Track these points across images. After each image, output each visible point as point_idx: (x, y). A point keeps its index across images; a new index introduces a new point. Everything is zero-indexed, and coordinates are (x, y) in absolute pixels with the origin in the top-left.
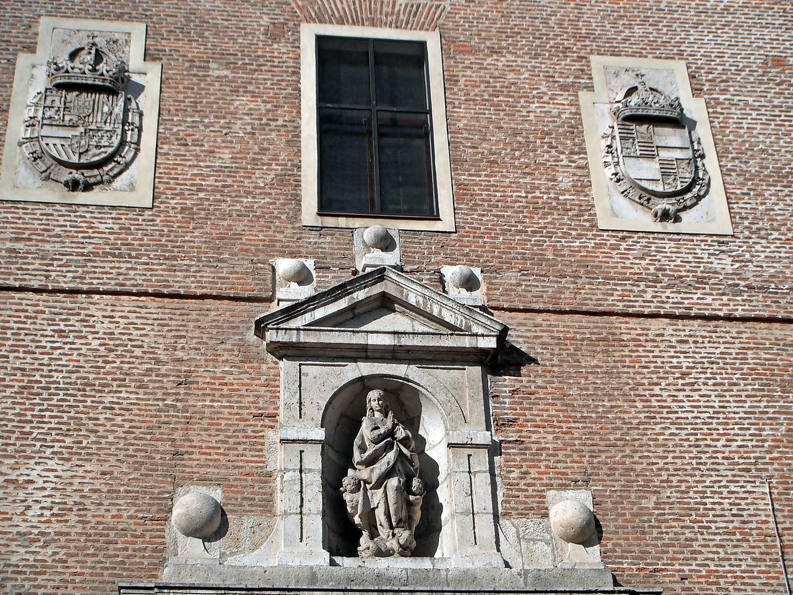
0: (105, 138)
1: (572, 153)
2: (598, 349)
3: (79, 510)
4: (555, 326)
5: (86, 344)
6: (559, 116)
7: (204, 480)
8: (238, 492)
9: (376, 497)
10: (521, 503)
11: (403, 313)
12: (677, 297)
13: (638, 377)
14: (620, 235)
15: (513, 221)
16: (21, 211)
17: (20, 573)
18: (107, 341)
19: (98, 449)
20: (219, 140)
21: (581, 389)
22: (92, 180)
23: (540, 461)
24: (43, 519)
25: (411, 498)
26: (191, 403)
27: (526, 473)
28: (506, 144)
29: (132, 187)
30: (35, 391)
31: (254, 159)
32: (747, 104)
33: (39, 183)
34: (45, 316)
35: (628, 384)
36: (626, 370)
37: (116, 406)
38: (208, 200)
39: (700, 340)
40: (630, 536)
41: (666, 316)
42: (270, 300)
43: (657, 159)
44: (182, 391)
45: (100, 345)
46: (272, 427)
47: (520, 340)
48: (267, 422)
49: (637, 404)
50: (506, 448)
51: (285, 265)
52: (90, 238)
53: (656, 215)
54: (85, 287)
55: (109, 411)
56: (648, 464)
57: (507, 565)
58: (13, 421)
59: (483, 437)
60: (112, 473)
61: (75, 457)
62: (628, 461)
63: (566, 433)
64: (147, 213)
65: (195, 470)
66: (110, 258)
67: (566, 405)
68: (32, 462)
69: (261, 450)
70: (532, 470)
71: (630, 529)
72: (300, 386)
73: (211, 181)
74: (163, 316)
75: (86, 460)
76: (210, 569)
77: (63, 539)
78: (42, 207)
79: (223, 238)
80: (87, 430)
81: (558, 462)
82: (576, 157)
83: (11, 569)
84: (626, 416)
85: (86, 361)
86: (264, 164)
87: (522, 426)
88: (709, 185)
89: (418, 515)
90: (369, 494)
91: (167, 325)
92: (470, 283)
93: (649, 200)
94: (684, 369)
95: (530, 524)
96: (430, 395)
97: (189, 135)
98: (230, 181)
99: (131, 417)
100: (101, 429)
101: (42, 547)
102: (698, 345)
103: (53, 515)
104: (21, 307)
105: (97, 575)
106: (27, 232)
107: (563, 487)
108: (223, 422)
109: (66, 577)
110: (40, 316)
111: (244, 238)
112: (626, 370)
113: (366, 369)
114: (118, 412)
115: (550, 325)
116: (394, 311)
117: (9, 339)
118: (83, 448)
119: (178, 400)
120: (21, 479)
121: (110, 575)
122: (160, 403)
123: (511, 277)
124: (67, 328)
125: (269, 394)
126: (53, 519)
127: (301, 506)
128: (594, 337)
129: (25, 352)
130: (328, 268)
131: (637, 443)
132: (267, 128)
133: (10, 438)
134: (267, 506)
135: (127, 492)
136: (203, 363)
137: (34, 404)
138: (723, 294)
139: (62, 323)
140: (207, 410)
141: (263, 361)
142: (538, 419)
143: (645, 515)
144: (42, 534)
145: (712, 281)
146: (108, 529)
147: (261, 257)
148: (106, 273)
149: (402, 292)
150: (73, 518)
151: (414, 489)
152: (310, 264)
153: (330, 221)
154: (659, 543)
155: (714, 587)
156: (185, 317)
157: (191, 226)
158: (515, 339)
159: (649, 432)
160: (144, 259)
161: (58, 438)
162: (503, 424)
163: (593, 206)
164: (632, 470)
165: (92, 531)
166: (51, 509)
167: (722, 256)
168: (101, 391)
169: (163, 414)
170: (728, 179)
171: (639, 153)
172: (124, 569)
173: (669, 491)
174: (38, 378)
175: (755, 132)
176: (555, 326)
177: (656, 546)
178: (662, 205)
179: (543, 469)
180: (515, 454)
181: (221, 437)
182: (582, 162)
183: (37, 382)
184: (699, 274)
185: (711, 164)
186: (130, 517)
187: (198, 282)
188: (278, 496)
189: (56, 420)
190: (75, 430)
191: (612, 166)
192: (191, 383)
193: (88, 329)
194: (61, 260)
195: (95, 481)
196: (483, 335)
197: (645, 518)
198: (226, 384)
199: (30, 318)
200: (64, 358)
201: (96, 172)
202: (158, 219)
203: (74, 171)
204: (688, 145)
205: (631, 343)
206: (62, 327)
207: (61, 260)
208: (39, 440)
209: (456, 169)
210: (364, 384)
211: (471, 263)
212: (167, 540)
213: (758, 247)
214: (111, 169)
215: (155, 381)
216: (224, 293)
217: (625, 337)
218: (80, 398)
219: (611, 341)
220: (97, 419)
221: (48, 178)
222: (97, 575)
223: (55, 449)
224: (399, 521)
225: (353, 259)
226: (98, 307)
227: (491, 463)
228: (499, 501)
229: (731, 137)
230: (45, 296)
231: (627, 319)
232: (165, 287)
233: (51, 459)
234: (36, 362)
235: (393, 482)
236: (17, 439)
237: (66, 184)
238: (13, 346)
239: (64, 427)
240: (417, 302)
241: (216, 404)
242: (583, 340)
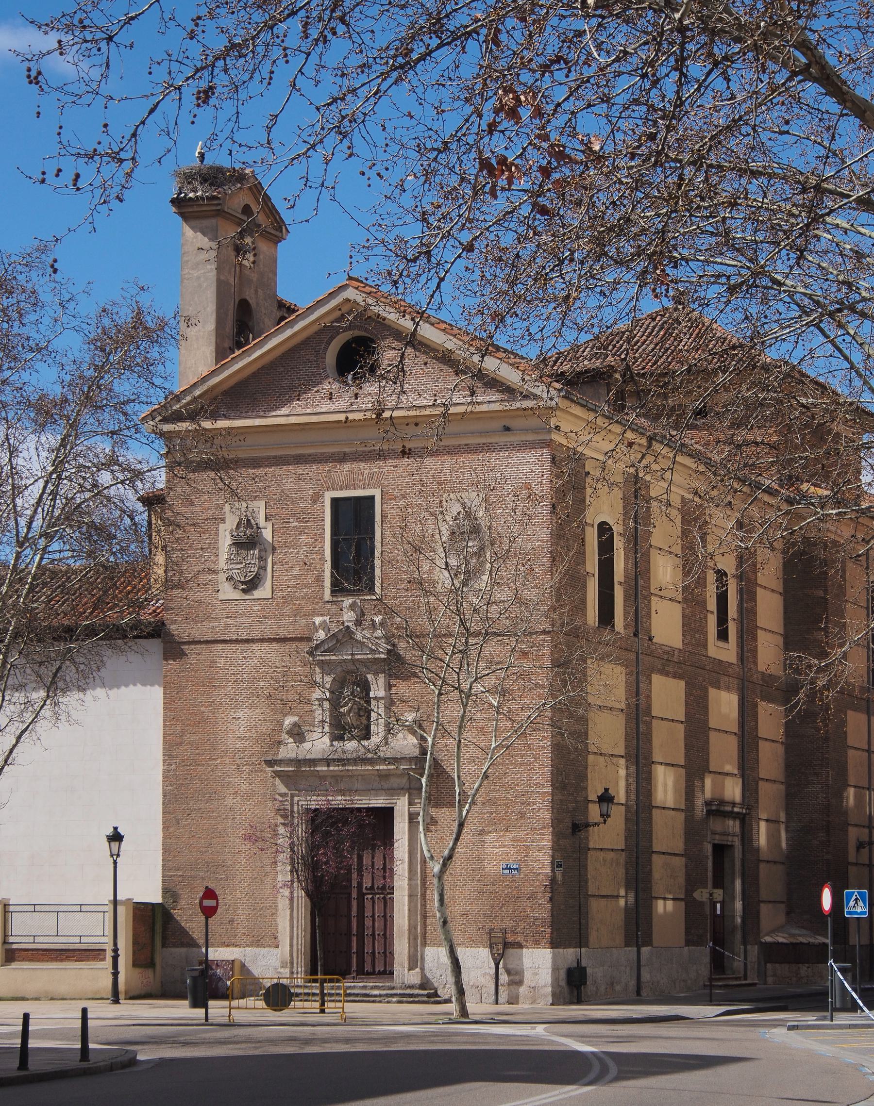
33: (233, 590)
150: (254, 731)
153: (335, 599)
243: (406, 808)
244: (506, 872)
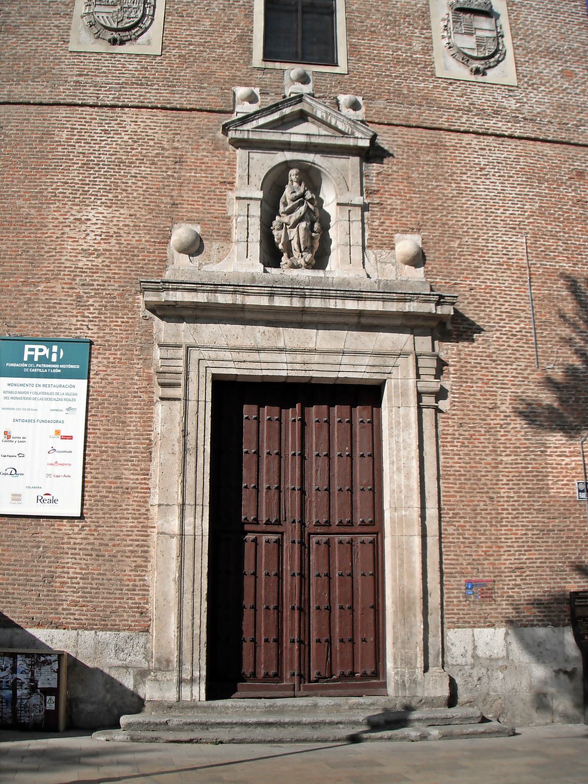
0: (133, 13)
1: (422, 29)
2: (431, 150)
3: (117, 236)
4: (406, 135)
5: (121, 138)
6: (416, 5)
7: (190, 220)
8: (210, 228)
9: (293, 233)
10: (379, 240)
11: (313, 122)
12: (481, 122)
13: (454, 168)
14: (449, 81)
15: (384, 69)
16: (82, 58)
17: (83, 272)
18: (133, 136)
19: (128, 201)
20: (203, 13)
21: (420, 174)
22: (125, 38)
23: (392, 216)
24: (96, 242)
25: (313, 234)
26: (183, 174)
27: (383, 223)
28: (381, 21)
29: (149, 43)
30: (91, 166)
31: (224, 26)
32: (531, 6)
33: (93, 40)
34: (96, 121)
35: (447, 172)
36: (447, 164)
37: (138, 175)
38: (195, 50)
39: (493, 149)
40: (442, 263)
41: (473, 133)
42: (232, 112)
43: (475, 36)
44: (177, 167)
45: (129, 138)
46: (231, 190)
47: (384, 142)
48: (228, 186)
49: (453, 185)
50: (372, 207)
51: (241, 91)
52: (123, 73)
53: (471, 71)
54: (120, 104)
55: (134, 179)
56: (456, 221)
57: (368, 276)
58: (78, 184)
59: (358, 200)
60: (136, 215)
61: (114, 206)
62: (444, 218)
63: (408, 200)
64: (158, 58)
65: (185, 214)
66: (135, 86)
67: (410, 183)
68: (89, 208)
69: (224, 203)
70: (387, 221)
71: (442, 259)
72: (249, 165)
73: (197, 39)
74: (167, 122)
75: (120, 207)
76: (193, 272)
77: (107, 253)
78: (95, 55)
79: (204, 74)
80: (121, 190)
81: (403, 217)
82: (425, 31)
83: (78, 270)
84: (445, 192)
85: (120, 148)
86: (230, 29)
87: (382, 194)
88: (505, 54)
89: (317, 245)
90: (288, 231)
91: (169, 127)
92: (355, 106)
93: (468, 61)
94: (482, 166)
96: (327, 174)
97: (184, 10)
98: (209, 39)
99: (147, 182)
100: (129, 189)
101: (96, 258)
103: (102, 239)
104: (82, 116)
105: (127, 274)
106: (86, 71)
107: (405, 232)
108: (202, 186)
109: (110, 275)
110: (94, 121)
111: (217, 74)
112: (447, 164)
113: (289, 156)
114: (139, 179)
115: (403, 134)
116: (308, 121)
117: (75, 135)
118: (118, 200)
119: (175, 172)
120: (83, 218)
121: (135, 275)
122: (164, 174)
123: (380, 103)
124: (109, 129)
125: (229, 170)
126: (102, 241)
127: (247, 237)
128: (429, 143)
129: (85, 143)
130: (268, 94)
131: (450, 208)
132: (233, 6)
133: (76, 194)
134: (227, 236)
135: (144, 226)
136: (190, 150)
137: (90, 174)
138: (509, 122)
139: (106, 126)
140: (192, 179)
141: (227, 149)
142: (392, 190)
143: (452, 251)
144: (96, 250)
145: (503, 113)
146: (134, 248)
147: (227, 86)
148: (133, 95)
149: (313, 110)
150: (113, 241)
151: (315, 229)
152: (257, 91)
153: (270, 65)
154: (459, 268)
155: (488, 295)
156: (180, 122)
157: (185, 66)
158: (383, 142)
159: (458, 202)
160: (155, 87)
161: (104, 194)
162: (371, 193)
163: (433, 62)
164: (446, 224)
165: (125, 249)
166: (101, 236)
167: (510, 98)
168: (129, 166)
169: (166, 180)
170: (517, 51)
171: (463, 31)
172: (143, 271)
173: (467, 237)
174: (92, 158)
175: (535, 24)
176: (406, 135)
177: (457, 269)
178: (476, 64)
179: (393, 221)
180: (377, 211)
181: (201, 195)
182: (428, 35)
183: (91, 161)
184: (496, 109)
185: (507, 42)
186: (147, 241)
187: (188, 101)
188: (234, 231)
189: (103, 183)
190: (114, 189)
191: (447, 39)
192: (183, 162)
193: (122, 129)
194: (106, 87)
195: (126, 220)
196: (361, 138)
197: (452, 253)
198: (204, 163)
199: (88, 122)
200: (108, 146)
201: (127, 33)
202: (165, 62)
203: (114, 33)
204: (494, 28)
205: (452, 148)
206: (106, 128)
207: (106, 87)
208: (93, 195)
209: (350, 35)
210: (287, 165)
211: (357, 94)
212: (168, 255)
213: (532, 95)
214: (137, 32)
215: (161, 161)
216: (204, 107)
217: (448, 144)
218: (117, 170)
219: (439, 146)
220: (127, 183)
221: (98, 37)
222: (127, 274)
223: (103, 201)
224: (305, 248)
225: (283, 88)
226: (128, 116)
227: (363, 216)
228: (366, 239)
229: (521, 26)
230: (96, 109)
231: (450, 133)
232: (168, 103)
233: (101, 206)
234: (91, 149)
235: (303, 225)
236: (81, 194)
237: (109, 41)
238: (78, 139)
239: (108, 188)
240: (322, 116)
241: (197, 175)
242: (422, 144)
243: (412, 382)
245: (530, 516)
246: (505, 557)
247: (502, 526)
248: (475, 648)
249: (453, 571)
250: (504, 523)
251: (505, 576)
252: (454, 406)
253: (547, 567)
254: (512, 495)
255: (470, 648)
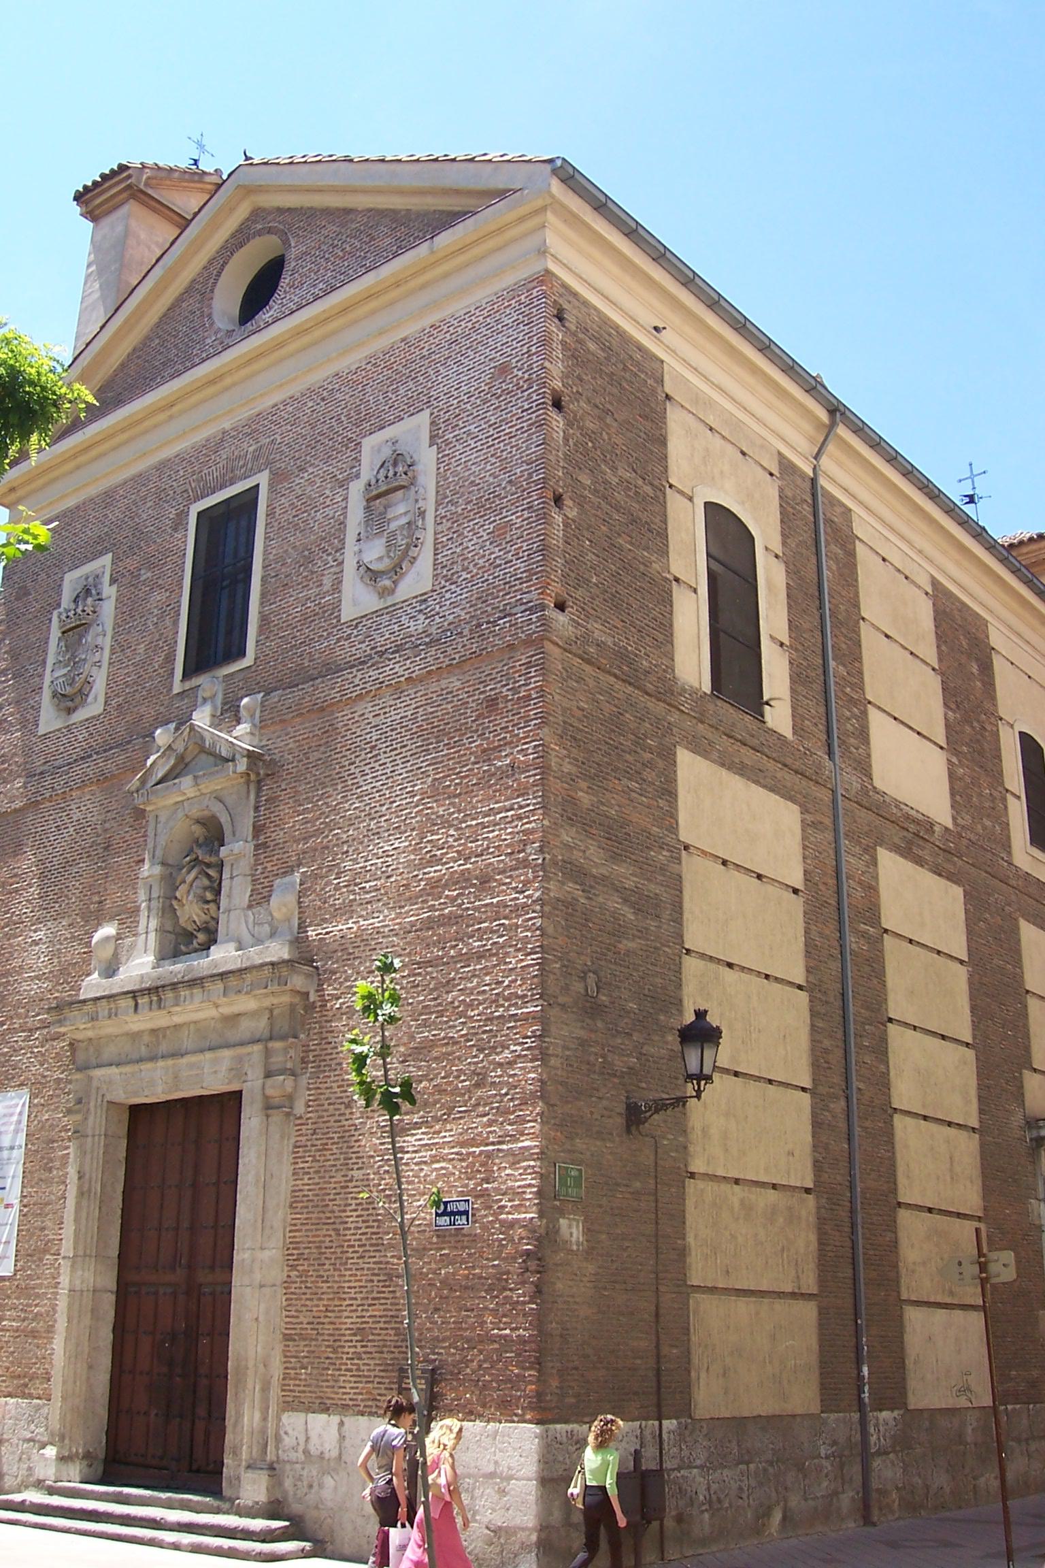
14: (354, 623)
32: (469, 433)
95: (262, 911)
102: (387, 715)
213: (448, 595)
244: (444, 1220)
245: (377, 1254)
246: (346, 1314)
247: (346, 1270)
248: (307, 1439)
249: (293, 1332)
250: (349, 1266)
251: (345, 1341)
252: (309, 1106)
253: (392, 1329)
254: (360, 1225)
255: (302, 1440)
